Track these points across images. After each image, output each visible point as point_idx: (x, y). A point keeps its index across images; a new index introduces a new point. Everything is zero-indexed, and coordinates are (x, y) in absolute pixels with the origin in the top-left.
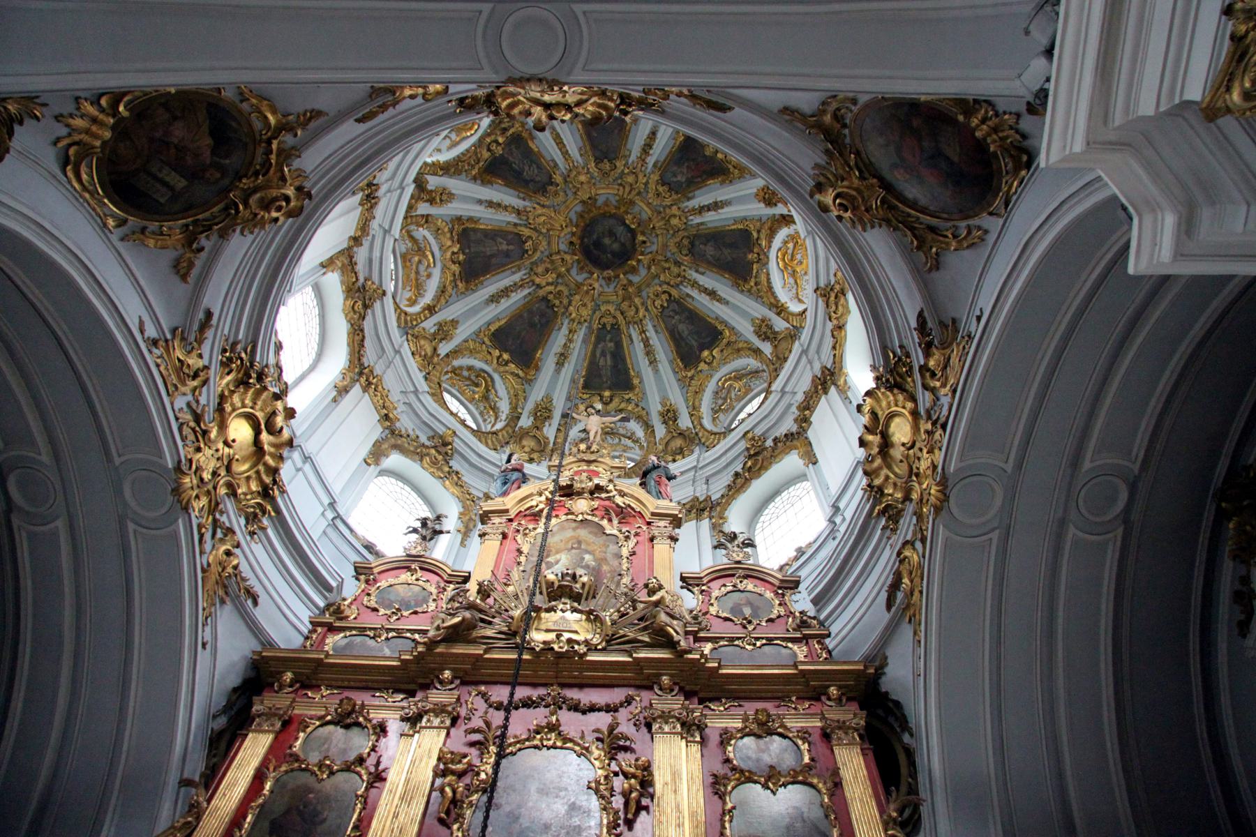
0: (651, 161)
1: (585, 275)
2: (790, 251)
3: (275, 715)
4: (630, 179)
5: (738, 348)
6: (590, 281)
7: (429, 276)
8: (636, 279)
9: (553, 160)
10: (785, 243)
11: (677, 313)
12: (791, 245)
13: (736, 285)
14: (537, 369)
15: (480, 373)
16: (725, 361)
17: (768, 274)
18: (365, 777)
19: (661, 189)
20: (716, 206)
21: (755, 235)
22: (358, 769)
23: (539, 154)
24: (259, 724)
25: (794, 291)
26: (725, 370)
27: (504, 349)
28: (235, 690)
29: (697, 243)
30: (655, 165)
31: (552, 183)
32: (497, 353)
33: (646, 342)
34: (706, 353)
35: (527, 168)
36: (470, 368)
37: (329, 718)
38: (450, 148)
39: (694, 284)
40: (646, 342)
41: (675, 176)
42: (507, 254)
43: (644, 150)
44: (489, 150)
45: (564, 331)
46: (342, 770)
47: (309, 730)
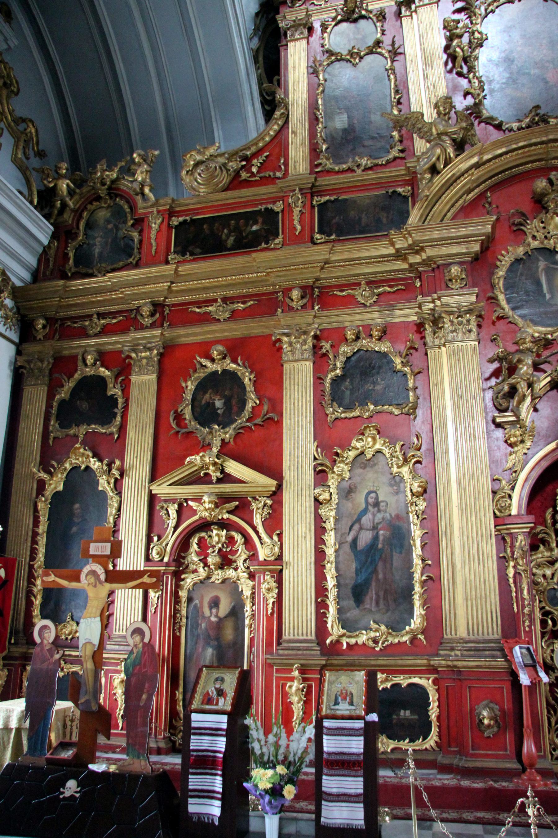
3: (300, 25)
18: (387, 55)
22: (379, 50)
24: (292, 35)
28: (257, 14)
37: (339, 18)
46: (367, 54)
47: (328, 30)
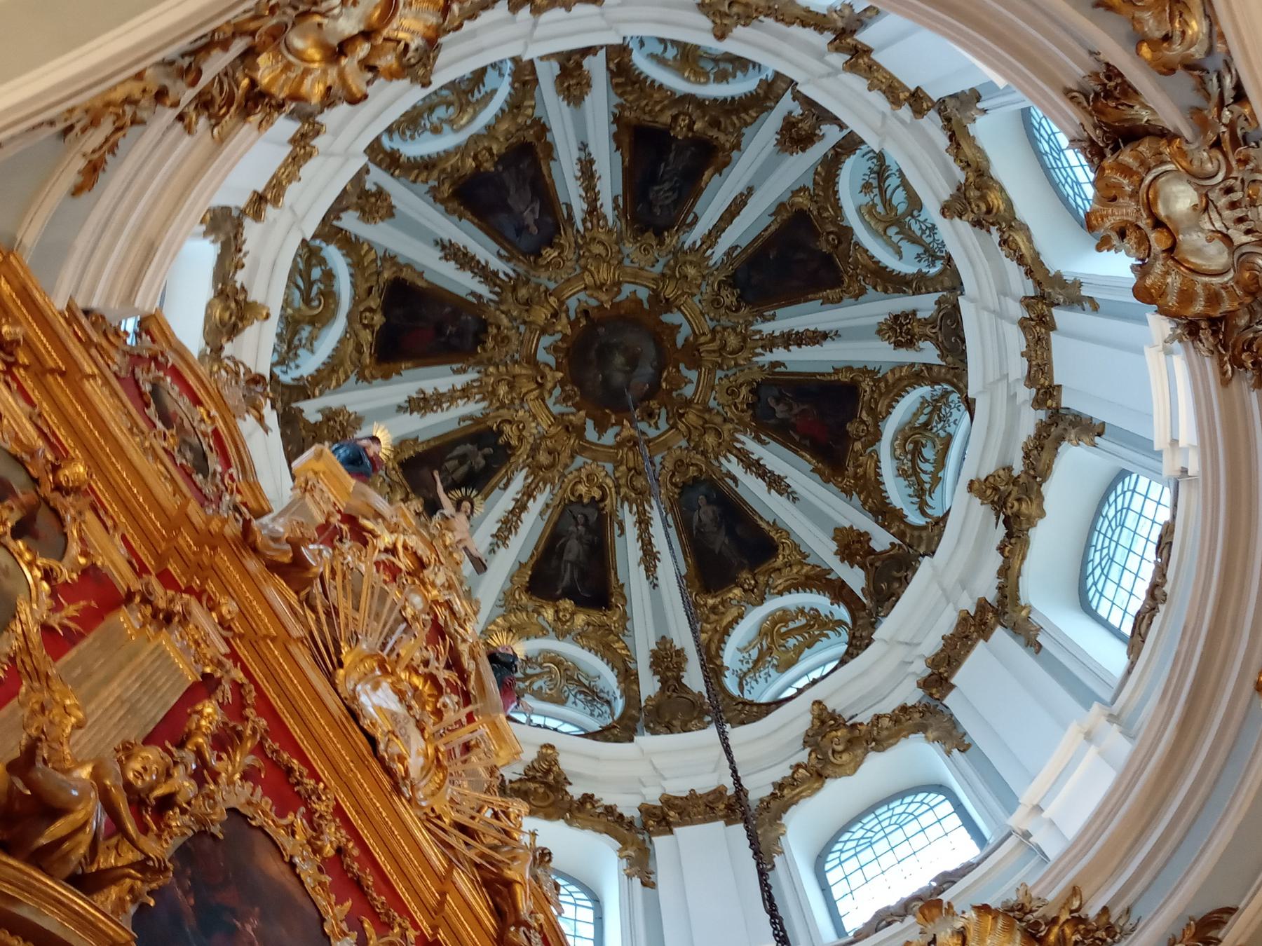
0: (779, 354)
1: (551, 360)
2: (791, 625)
4: (733, 341)
5: (609, 643)
6: (547, 370)
7: (436, 130)
8: (591, 434)
9: (696, 219)
10: (801, 611)
11: (586, 524)
12: (802, 621)
13: (685, 583)
14: (386, 377)
15: (329, 295)
16: (581, 637)
17: (741, 616)
19: (744, 391)
20: (776, 483)
21: (780, 561)
23: (698, 193)
25: (745, 668)
26: (568, 649)
27: (386, 309)
29: (703, 489)
30: (775, 364)
31: (659, 234)
32: (374, 302)
33: (521, 507)
34: (567, 604)
35: (666, 186)
36: (329, 276)
38: (652, 56)
39: (643, 523)
40: (521, 507)
41: (778, 401)
42: (521, 229)
43: (789, 334)
44: (675, 118)
45: (460, 381)
